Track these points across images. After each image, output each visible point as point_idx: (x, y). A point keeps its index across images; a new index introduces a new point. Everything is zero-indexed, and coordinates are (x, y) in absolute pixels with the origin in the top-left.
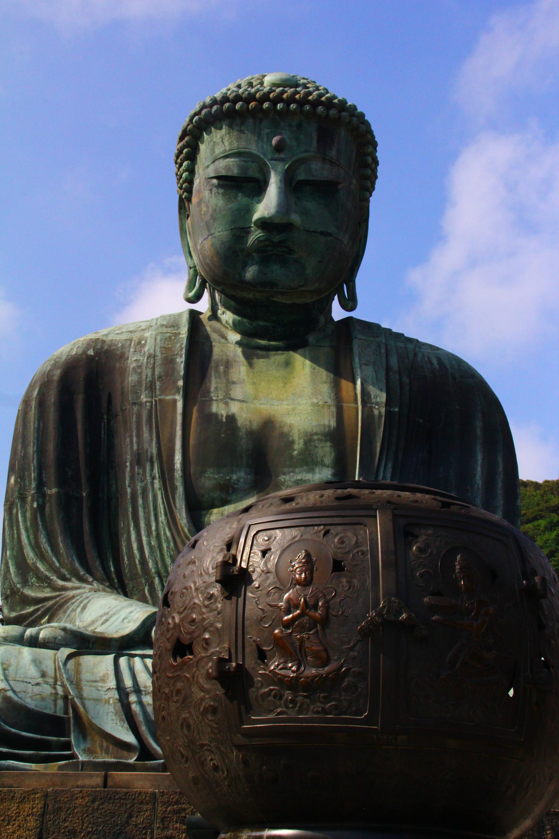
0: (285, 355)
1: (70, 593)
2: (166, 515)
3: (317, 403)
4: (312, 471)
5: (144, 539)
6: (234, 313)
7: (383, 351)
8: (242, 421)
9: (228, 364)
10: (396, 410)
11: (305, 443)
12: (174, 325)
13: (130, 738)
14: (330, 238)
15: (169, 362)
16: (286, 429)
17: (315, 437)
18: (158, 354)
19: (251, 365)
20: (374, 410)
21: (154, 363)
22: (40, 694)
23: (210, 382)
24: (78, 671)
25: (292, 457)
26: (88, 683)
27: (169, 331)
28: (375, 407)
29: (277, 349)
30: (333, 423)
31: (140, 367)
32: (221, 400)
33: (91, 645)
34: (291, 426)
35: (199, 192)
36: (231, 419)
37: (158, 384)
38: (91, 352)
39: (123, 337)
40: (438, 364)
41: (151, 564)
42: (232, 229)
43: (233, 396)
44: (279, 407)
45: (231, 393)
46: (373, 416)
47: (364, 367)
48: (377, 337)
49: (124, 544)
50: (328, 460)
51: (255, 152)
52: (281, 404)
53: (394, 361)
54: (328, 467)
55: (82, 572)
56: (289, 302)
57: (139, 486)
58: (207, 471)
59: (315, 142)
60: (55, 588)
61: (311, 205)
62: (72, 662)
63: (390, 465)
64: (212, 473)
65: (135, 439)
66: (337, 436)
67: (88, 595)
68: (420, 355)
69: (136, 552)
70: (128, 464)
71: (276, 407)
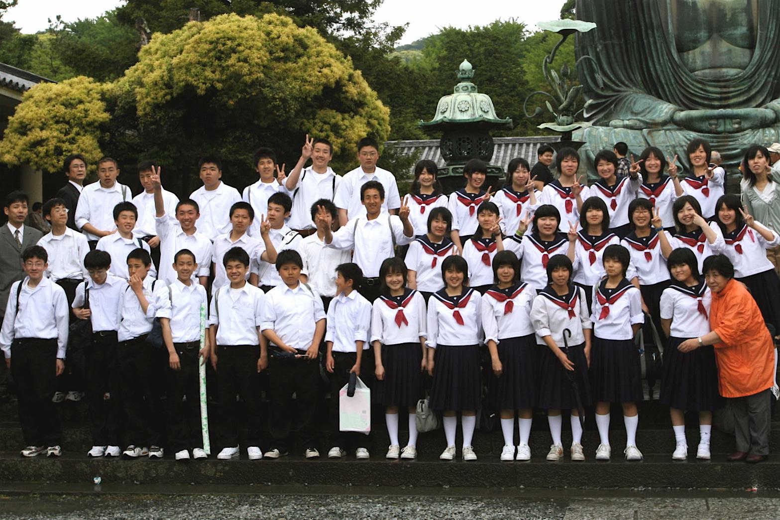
1: (624, 94)
2: (667, 55)
4: (736, 29)
5: (657, 67)
11: (733, 15)
16: (722, 7)
34: (725, 5)
49: (644, 67)
50: (745, 22)
57: (651, 40)
63: (775, 21)
65: (646, 16)
66: (748, 10)
67: (635, 95)
69: (654, 74)
70: (643, 28)
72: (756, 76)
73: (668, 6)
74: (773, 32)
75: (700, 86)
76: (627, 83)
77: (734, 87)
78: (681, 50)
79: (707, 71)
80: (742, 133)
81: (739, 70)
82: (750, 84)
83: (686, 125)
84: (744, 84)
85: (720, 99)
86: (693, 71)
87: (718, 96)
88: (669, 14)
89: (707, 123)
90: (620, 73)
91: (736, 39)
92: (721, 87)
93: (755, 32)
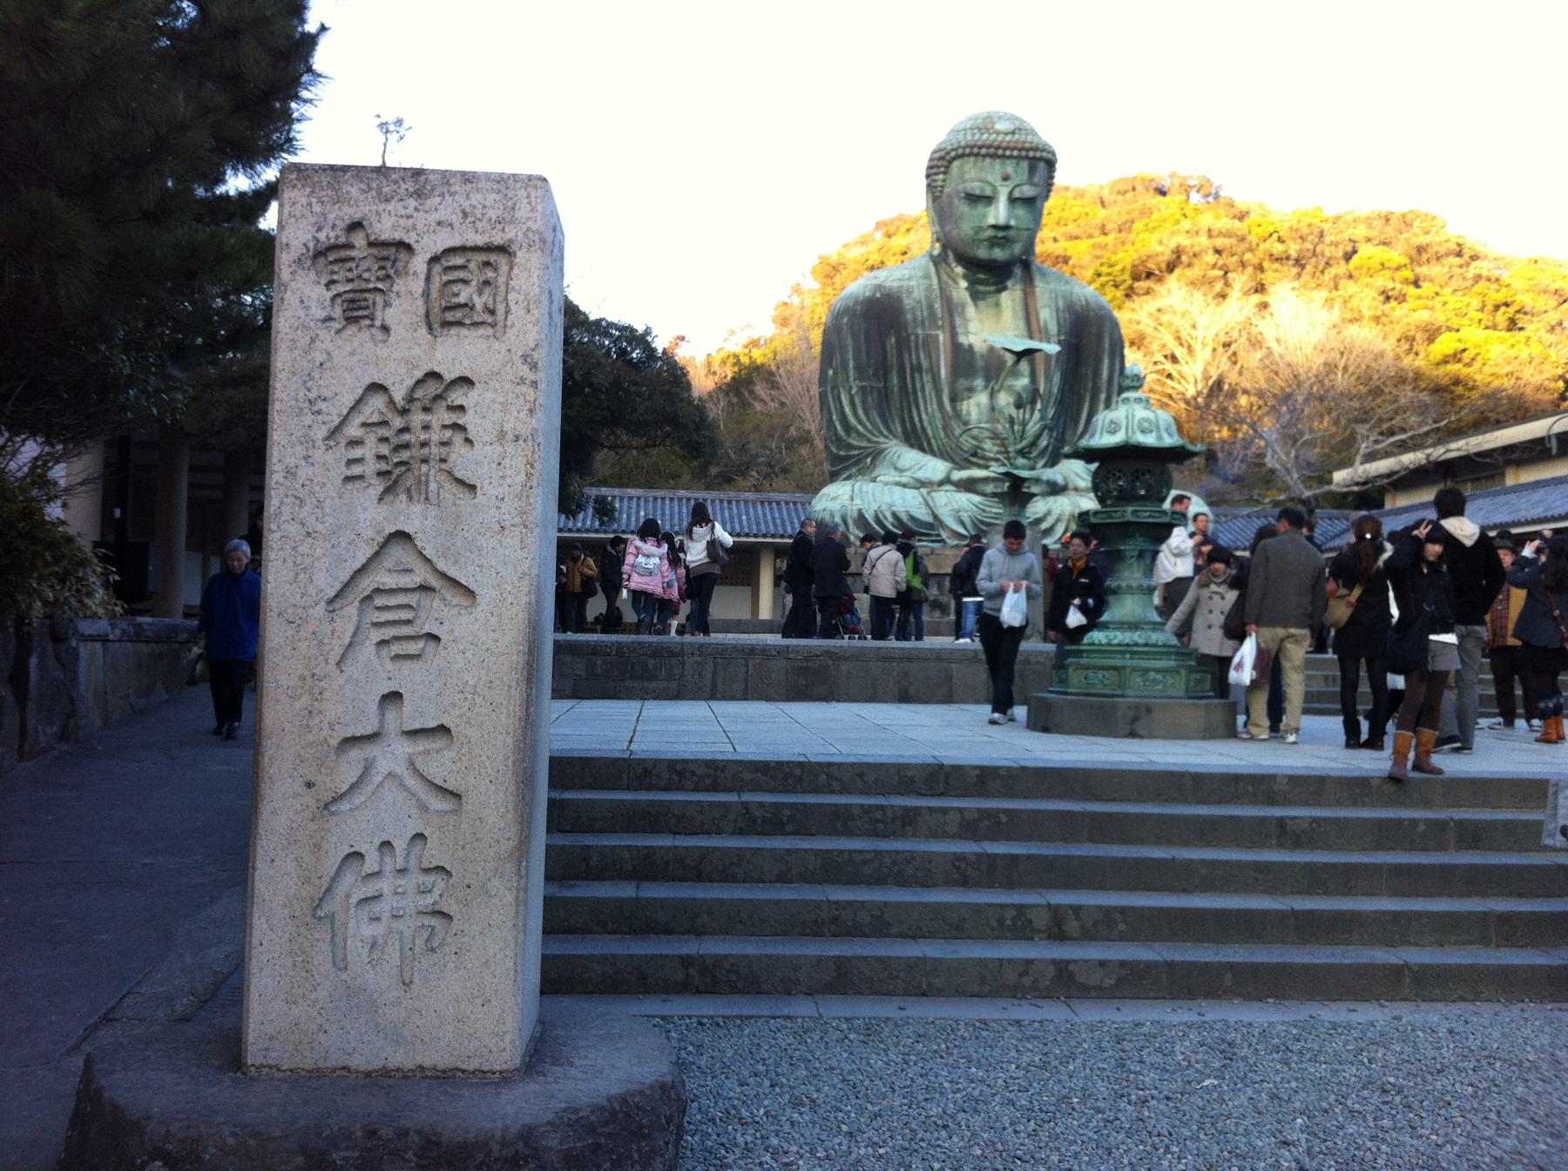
9: (963, 306)
13: (964, 532)
15: (931, 307)
35: (949, 196)
36: (971, 346)
39: (895, 284)
41: (929, 431)
53: (1061, 303)
60: (869, 440)
61: (1021, 211)
83: (968, 486)
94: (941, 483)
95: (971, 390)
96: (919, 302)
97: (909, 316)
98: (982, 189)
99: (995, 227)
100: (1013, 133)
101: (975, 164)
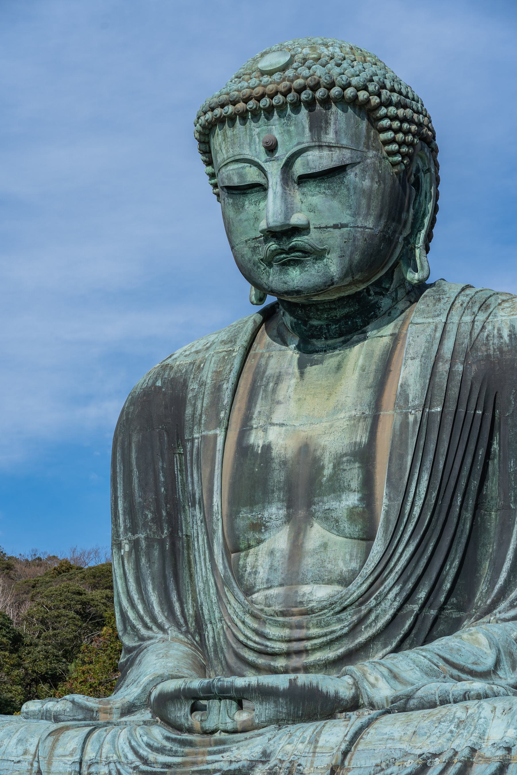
0: (340, 356)
3: (355, 416)
4: (338, 498)
6: (291, 316)
7: (438, 335)
8: (277, 449)
9: (278, 379)
10: (439, 409)
11: (334, 467)
12: (233, 339)
14: (345, 229)
15: (217, 389)
16: (318, 453)
17: (345, 459)
18: (209, 381)
19: (302, 374)
20: (410, 416)
21: (204, 393)
22: (18, 771)
23: (256, 404)
24: (53, 748)
25: (321, 485)
26: (58, 758)
27: (225, 350)
28: (411, 412)
29: (335, 348)
30: (365, 440)
31: (195, 397)
32: (261, 427)
33: (95, 715)
34: (324, 449)
36: (267, 448)
37: (204, 417)
38: (159, 384)
39: (189, 360)
40: (510, 336)
42: (246, 241)
43: (275, 420)
44: (318, 425)
45: (272, 416)
46: (408, 423)
47: (409, 362)
48: (438, 315)
50: (355, 484)
51: (249, 157)
52: (321, 422)
54: (355, 491)
55: (161, 618)
56: (335, 297)
58: (240, 511)
59: (307, 130)
62: (51, 739)
63: (425, 477)
64: (246, 513)
68: (489, 327)
71: (316, 426)
72: (372, 602)
73: (218, 456)
74: (419, 503)
75: (255, 625)
76: (161, 618)
77: (318, 625)
78: (235, 547)
79: (273, 592)
80: (256, 732)
81: (337, 588)
82: (355, 618)
84: (340, 620)
85: (288, 654)
86: (249, 591)
87: (284, 646)
88: (217, 472)
89: (187, 709)
90: (154, 599)
91: (337, 521)
92: (291, 627)
93: (378, 503)
94: (129, 709)
95: (259, 527)
96: (202, 384)
97: (189, 411)
98: (241, 176)
99: (271, 234)
100: (284, 68)
101: (225, 135)
